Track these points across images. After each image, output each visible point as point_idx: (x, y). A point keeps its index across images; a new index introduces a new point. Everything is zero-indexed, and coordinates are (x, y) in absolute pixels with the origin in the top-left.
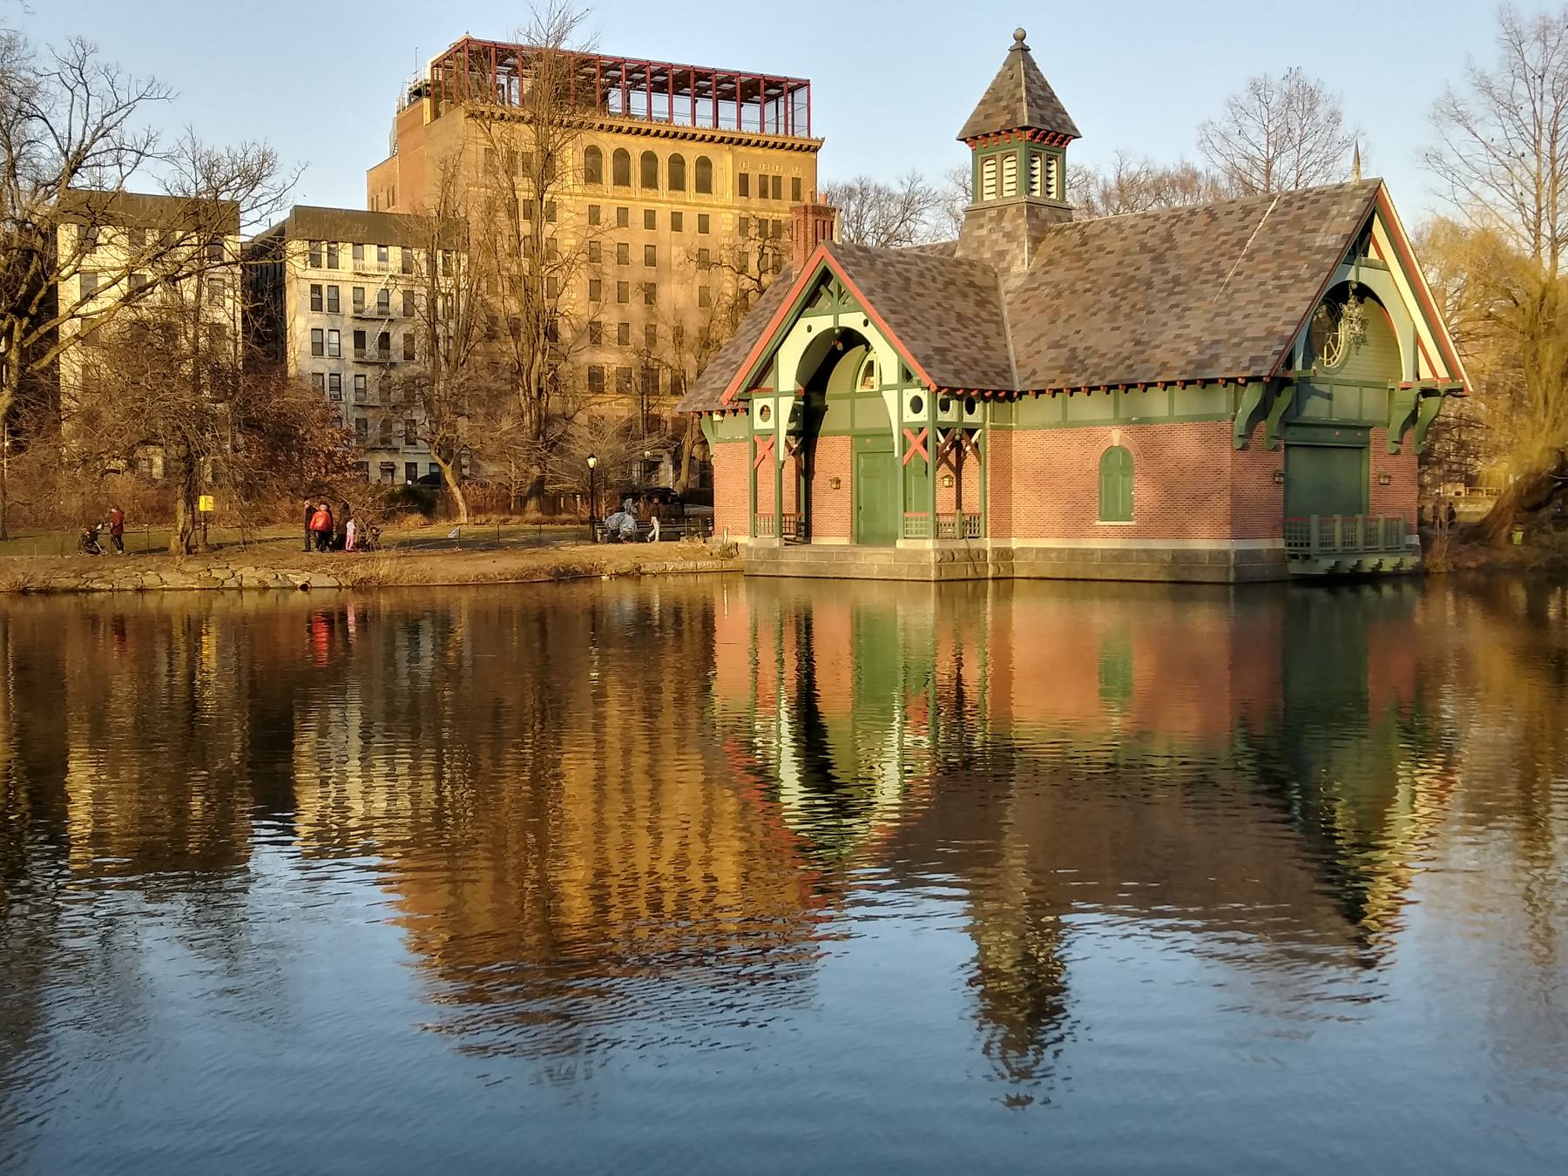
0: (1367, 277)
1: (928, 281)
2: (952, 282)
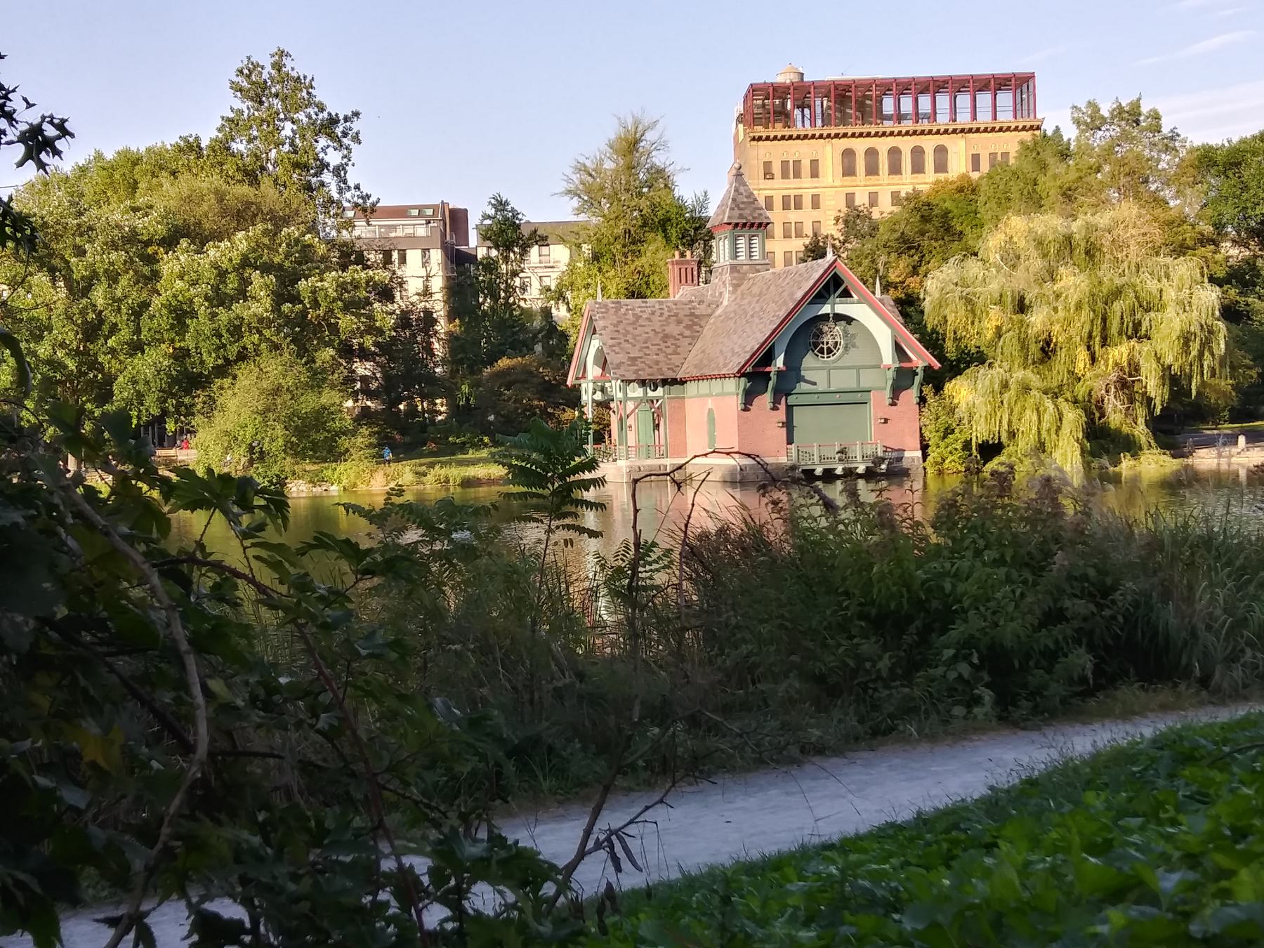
0: (842, 308)
1: (656, 318)
2: (676, 315)
